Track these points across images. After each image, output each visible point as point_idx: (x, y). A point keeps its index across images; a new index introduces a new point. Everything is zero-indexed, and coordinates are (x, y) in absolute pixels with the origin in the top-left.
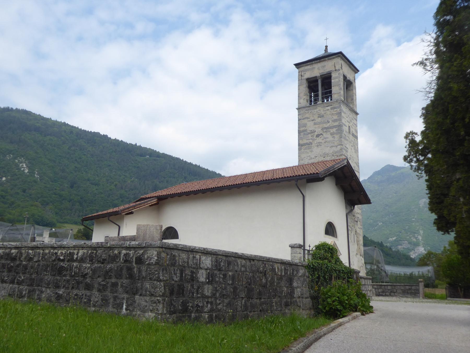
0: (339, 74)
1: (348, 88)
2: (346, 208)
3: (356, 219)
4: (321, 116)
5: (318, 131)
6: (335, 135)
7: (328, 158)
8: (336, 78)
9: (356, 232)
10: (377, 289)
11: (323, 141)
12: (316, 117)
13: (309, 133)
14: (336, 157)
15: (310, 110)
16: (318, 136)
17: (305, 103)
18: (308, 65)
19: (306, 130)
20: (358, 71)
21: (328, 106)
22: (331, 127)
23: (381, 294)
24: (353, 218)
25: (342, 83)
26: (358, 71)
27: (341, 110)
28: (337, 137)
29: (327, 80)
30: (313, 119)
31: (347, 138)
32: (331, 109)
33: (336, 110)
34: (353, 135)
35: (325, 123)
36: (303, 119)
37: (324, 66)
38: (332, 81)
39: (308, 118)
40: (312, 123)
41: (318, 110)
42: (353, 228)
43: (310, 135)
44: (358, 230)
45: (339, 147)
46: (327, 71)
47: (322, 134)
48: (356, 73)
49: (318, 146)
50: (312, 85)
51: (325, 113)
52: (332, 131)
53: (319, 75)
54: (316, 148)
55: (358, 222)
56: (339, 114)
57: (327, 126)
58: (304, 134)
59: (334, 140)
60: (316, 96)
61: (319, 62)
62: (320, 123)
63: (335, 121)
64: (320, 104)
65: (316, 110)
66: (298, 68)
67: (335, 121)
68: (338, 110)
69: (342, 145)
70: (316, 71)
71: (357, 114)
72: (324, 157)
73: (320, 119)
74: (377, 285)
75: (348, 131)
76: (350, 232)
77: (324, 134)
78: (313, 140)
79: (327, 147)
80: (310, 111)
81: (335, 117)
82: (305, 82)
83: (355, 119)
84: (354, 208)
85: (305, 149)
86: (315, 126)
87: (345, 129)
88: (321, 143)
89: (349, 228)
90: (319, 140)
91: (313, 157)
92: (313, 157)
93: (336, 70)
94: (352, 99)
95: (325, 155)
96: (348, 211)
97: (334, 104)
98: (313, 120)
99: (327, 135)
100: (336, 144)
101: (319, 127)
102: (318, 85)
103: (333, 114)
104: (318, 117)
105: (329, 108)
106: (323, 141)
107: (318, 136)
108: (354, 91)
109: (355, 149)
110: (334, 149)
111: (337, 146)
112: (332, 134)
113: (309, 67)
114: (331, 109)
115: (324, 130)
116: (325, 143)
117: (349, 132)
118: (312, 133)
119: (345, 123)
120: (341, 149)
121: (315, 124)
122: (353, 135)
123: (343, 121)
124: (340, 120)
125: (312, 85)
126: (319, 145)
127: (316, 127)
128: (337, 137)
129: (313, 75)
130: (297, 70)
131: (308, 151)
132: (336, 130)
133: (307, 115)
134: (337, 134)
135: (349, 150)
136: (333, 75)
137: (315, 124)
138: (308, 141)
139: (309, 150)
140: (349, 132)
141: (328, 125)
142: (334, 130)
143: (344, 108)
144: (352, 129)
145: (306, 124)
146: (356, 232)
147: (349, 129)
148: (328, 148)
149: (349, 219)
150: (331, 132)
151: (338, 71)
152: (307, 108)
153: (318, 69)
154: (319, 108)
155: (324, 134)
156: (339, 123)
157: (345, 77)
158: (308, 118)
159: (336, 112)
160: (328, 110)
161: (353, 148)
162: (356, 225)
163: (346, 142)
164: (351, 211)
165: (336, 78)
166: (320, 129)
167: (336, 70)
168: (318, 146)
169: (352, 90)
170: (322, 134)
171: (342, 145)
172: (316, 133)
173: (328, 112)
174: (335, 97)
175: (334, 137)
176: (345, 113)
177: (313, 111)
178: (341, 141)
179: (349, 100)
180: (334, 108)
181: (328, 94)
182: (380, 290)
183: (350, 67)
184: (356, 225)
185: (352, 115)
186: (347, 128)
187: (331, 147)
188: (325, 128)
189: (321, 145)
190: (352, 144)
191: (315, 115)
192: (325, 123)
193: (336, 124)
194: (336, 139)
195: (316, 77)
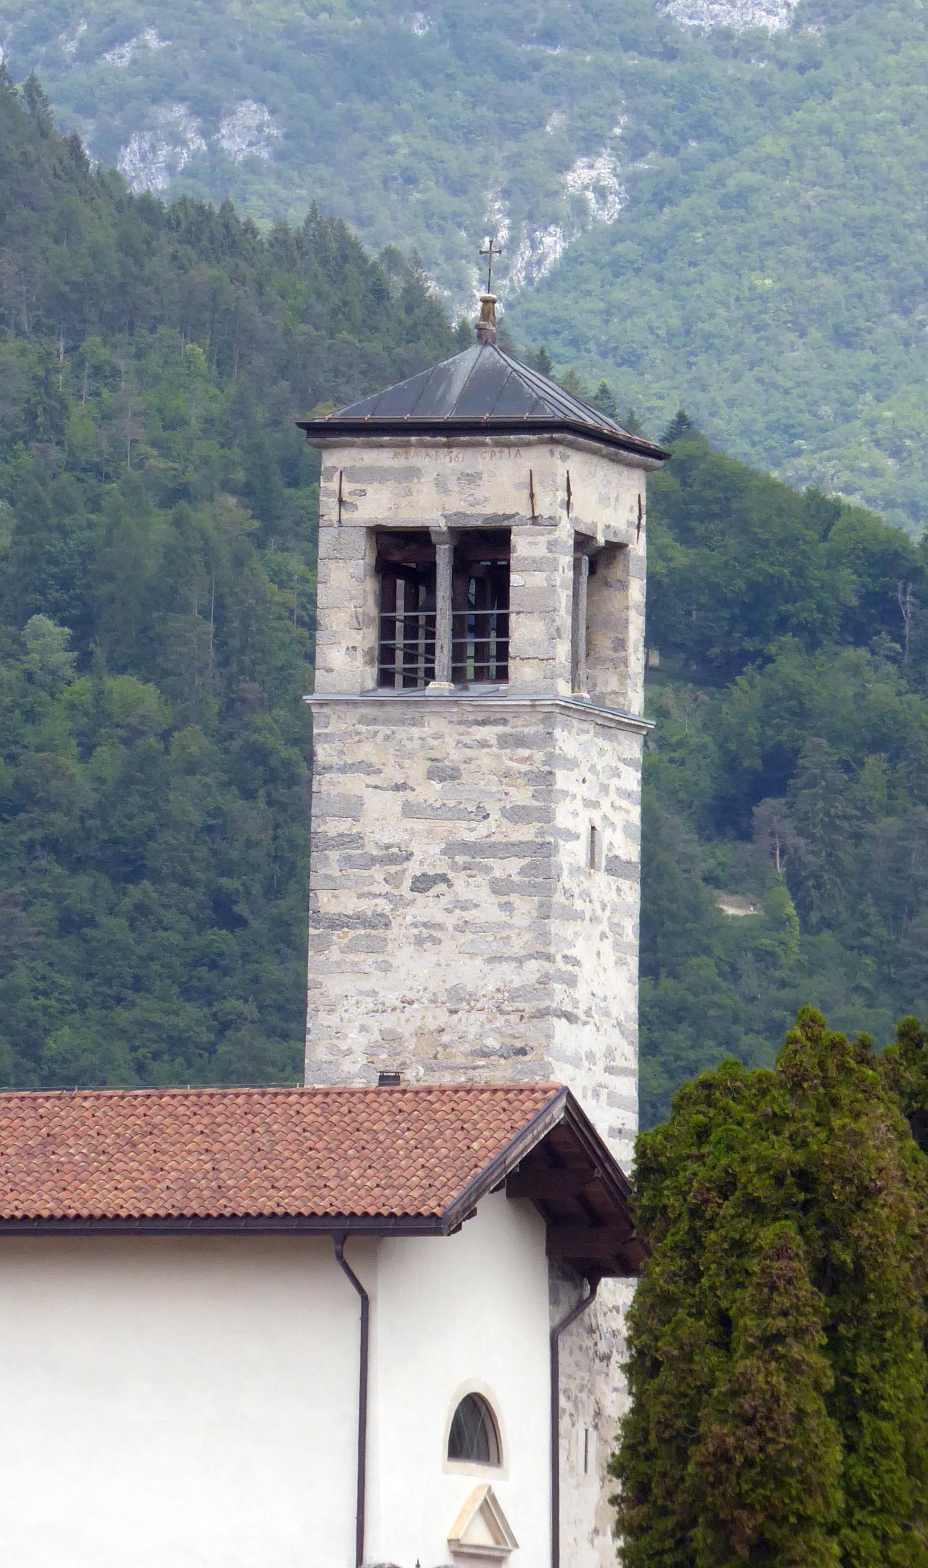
2: (554, 1300)
4: (442, 772)
5: (427, 855)
6: (514, 898)
7: (471, 1024)
8: (536, 565)
9: (598, 1414)
11: (450, 921)
12: (416, 770)
13: (374, 860)
14: (514, 1018)
15: (386, 722)
16: (423, 884)
21: (483, 723)
22: (493, 846)
24: (589, 1343)
28: (525, 907)
36: (344, 769)
39: (368, 769)
40: (391, 802)
41: (427, 730)
42: (584, 1396)
43: (378, 873)
45: (533, 965)
47: (444, 879)
51: (468, 761)
54: (409, 950)
56: (543, 780)
57: (471, 837)
58: (348, 859)
63: (517, 815)
64: (441, 701)
65: (416, 731)
67: (517, 815)
68: (539, 756)
72: (454, 1012)
73: (437, 786)
77: (459, 880)
78: (398, 902)
79: (473, 955)
80: (384, 730)
81: (522, 796)
84: (593, 1292)
86: (409, 823)
88: (440, 927)
90: (427, 908)
93: (534, 519)
96: (564, 1310)
100: (517, 947)
101: (430, 831)
102: (433, 566)
104: (431, 775)
105: (489, 733)
106: (450, 921)
107: (423, 884)
110: (509, 975)
111: (520, 961)
115: (460, 859)
116: (457, 928)
118: (393, 860)
120: (545, 980)
121: (409, 811)
123: (563, 817)
124: (546, 816)
126: (427, 936)
127: (413, 833)
128: (525, 907)
132: (522, 871)
133: (367, 752)
134: (523, 890)
137: (409, 811)
142: (511, 867)
146: (598, 1414)
148: (478, 962)
149: (563, 1358)
150: (497, 873)
152: (364, 710)
154: (434, 725)
155: (459, 880)
156: (541, 833)
158: (368, 769)
159: (525, 768)
160: (484, 744)
162: (600, 1379)
164: (582, 1305)
165: (536, 565)
166: (435, 849)
168: (419, 941)
170: (444, 879)
171: (549, 958)
172: (414, 868)
173: (485, 759)
174: (522, 672)
175: (507, 907)
177: (402, 732)
178: (544, 936)
180: (519, 741)
181: (485, 651)
187: (492, 960)
188: (466, 848)
189: (437, 942)
191: (410, 755)
192: (458, 814)
193: (525, 833)
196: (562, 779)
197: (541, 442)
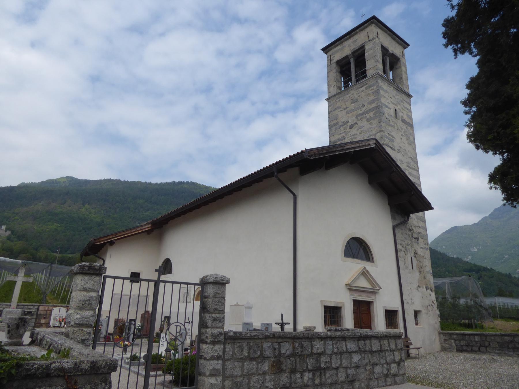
3: (415, 235)
4: (354, 101)
5: (352, 120)
6: (372, 121)
10: (458, 340)
16: (351, 127)
17: (334, 91)
18: (337, 45)
20: (408, 45)
23: (464, 348)
26: (408, 45)
27: (378, 86)
29: (360, 56)
30: (345, 107)
31: (392, 124)
32: (366, 88)
33: (372, 88)
34: (403, 121)
37: (355, 41)
38: (366, 54)
44: (420, 251)
46: (359, 45)
47: (356, 123)
48: (405, 48)
50: (344, 69)
52: (368, 116)
55: (420, 240)
57: (362, 112)
61: (350, 38)
65: (348, 96)
66: (326, 53)
70: (346, 49)
71: (410, 96)
74: (457, 334)
75: (393, 114)
76: (401, 254)
82: (334, 66)
83: (407, 102)
87: (389, 112)
88: (356, 134)
89: (399, 247)
94: (401, 78)
97: (369, 81)
103: (368, 94)
108: (403, 68)
109: (408, 139)
112: (368, 120)
113: (338, 48)
114: (366, 88)
115: (359, 118)
117: (396, 117)
119: (387, 104)
122: (403, 121)
125: (344, 69)
129: (343, 55)
130: (325, 56)
132: (374, 114)
136: (367, 47)
140: (396, 117)
141: (364, 109)
142: (371, 114)
143: (384, 85)
144: (400, 114)
147: (396, 113)
150: (368, 117)
151: (374, 44)
153: (350, 46)
154: (352, 92)
155: (360, 124)
157: (383, 47)
160: (363, 91)
161: (404, 138)
163: (390, 129)
166: (354, 118)
167: (369, 41)
169: (400, 67)
170: (356, 123)
173: (363, 94)
176: (386, 92)
179: (397, 80)
181: (362, 74)
182: (463, 343)
184: (415, 245)
185: (400, 96)
186: (392, 112)
190: (403, 133)
191: (347, 101)
193: (374, 105)
194: (374, 125)
195: (347, 57)
197: (369, 25)
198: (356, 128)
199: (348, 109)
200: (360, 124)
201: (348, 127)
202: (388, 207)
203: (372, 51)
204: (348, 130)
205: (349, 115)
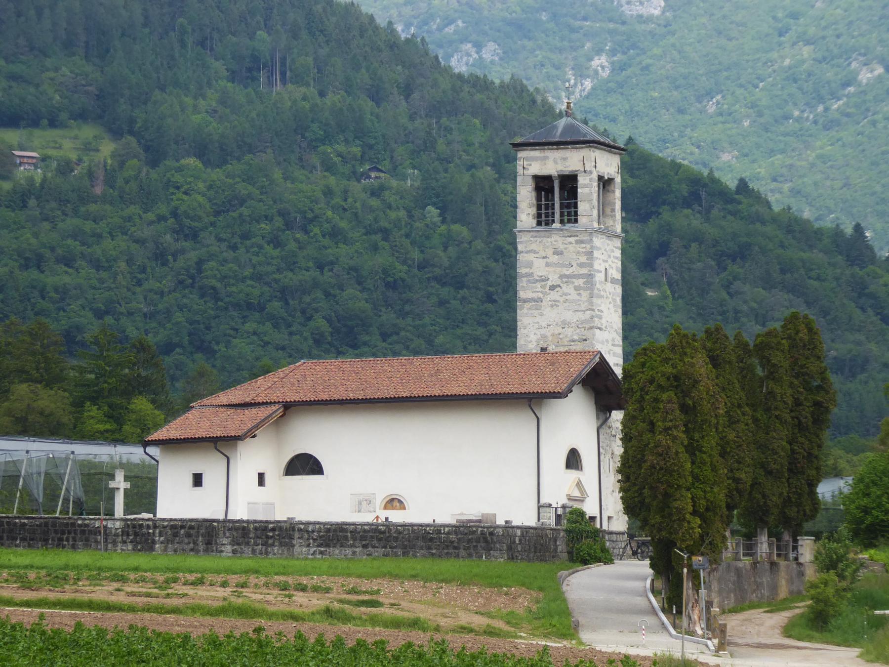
0: (591, 180)
1: (607, 187)
2: (598, 418)
4: (557, 252)
5: (554, 279)
6: (581, 292)
7: (569, 332)
8: (586, 186)
11: (561, 299)
12: (549, 252)
13: (537, 281)
14: (583, 329)
15: (540, 237)
16: (553, 288)
19: (531, 274)
24: (609, 431)
25: (595, 184)
28: (585, 294)
33: (584, 245)
35: (566, 266)
36: (527, 252)
37: (565, 159)
38: (579, 190)
39: (535, 252)
43: (538, 285)
45: (588, 312)
46: (570, 169)
47: (559, 286)
49: (552, 306)
53: (556, 174)
54: (549, 309)
57: (567, 273)
58: (529, 281)
59: (579, 300)
60: (550, 207)
62: (556, 265)
63: (582, 265)
64: (557, 230)
65: (549, 240)
67: (582, 265)
68: (588, 246)
69: (593, 310)
73: (556, 257)
76: (602, 457)
77: (564, 286)
78: (545, 294)
79: (569, 310)
80: (539, 240)
81: (583, 259)
85: (530, 309)
86: (547, 269)
88: (558, 301)
89: (601, 450)
90: (554, 295)
91: (544, 324)
92: (544, 324)
93: (585, 171)
95: (565, 324)
98: (544, 258)
99: (568, 289)
100: (583, 307)
102: (553, 187)
104: (554, 253)
105: (572, 239)
106: (561, 299)
107: (553, 288)
112: (577, 288)
114: (577, 242)
115: (564, 280)
116: (564, 302)
118: (543, 280)
120: (592, 317)
121: (548, 265)
123: (596, 266)
124: (591, 265)
126: (554, 304)
128: (585, 294)
131: (536, 312)
132: (584, 283)
133: (534, 247)
134: (585, 289)
135: (605, 314)
136: (582, 180)
137: (548, 265)
138: (535, 295)
139: (537, 312)
142: (580, 282)
145: (532, 262)
148: (571, 312)
150: (576, 284)
153: (555, 162)
155: (564, 286)
158: (535, 252)
160: (571, 243)
164: (607, 419)
165: (586, 186)
166: (557, 276)
168: (552, 306)
172: (549, 283)
173: (571, 248)
174: (582, 220)
175: (579, 294)
177: (545, 240)
178: (591, 303)
180: (582, 242)
181: (570, 214)
183: (610, 152)
187: (575, 311)
188: (566, 276)
189: (557, 306)
193: (584, 271)
196: (596, 254)
198: (559, 293)
199: (547, 260)
200: (565, 288)
201: (548, 288)
202: (594, 407)
203: (587, 190)
204: (547, 290)
205: (551, 269)
